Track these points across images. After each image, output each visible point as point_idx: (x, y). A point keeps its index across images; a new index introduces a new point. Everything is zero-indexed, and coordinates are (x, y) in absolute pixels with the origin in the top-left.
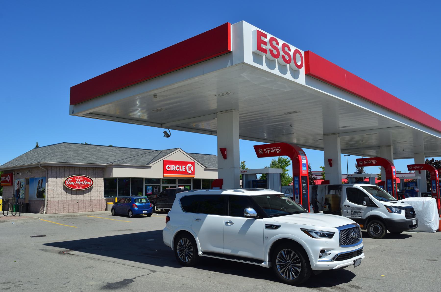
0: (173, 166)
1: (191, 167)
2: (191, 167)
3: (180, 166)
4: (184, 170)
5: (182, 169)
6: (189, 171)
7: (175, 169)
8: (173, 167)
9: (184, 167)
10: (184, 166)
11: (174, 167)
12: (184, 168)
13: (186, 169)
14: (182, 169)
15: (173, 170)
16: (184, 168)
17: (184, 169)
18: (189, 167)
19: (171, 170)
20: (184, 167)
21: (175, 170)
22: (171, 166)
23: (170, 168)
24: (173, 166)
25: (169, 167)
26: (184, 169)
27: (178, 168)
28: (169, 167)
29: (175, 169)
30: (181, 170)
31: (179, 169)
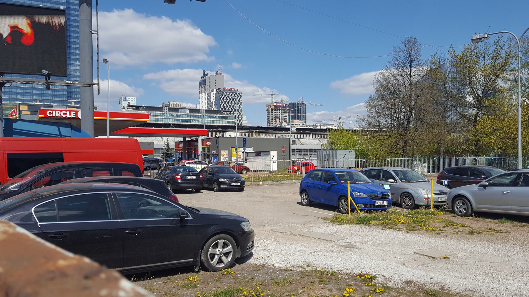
4: (75, 116)
5: (70, 114)
7: (60, 115)
9: (74, 113)
11: (58, 113)
12: (75, 114)
14: (70, 114)
15: (57, 116)
16: (75, 114)
17: (74, 115)
19: (54, 115)
20: (74, 113)
21: (60, 116)
23: (53, 114)
25: (50, 113)
26: (74, 115)
28: (50, 113)
29: (60, 115)
30: (70, 116)
31: (67, 115)
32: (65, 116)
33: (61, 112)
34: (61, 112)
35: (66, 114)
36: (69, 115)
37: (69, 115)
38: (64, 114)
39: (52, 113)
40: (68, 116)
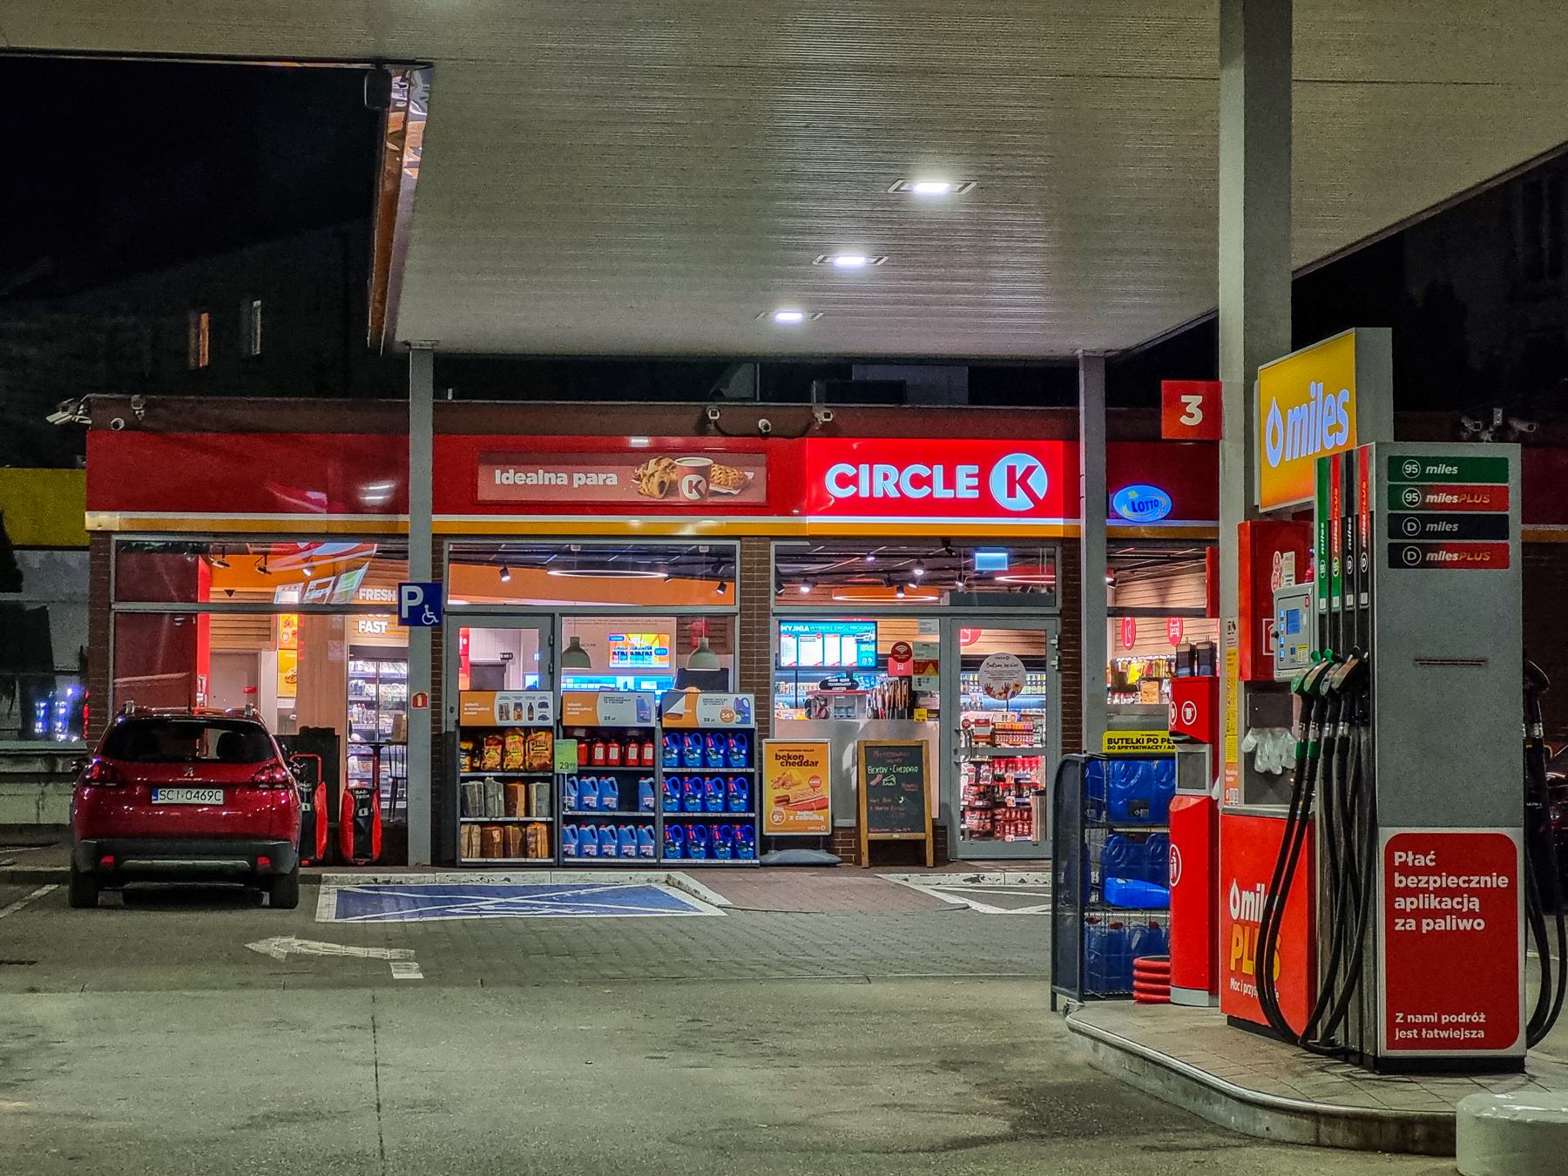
0: (879, 469)
1: (1030, 470)
2: (1030, 470)
3: (939, 471)
4: (975, 494)
5: (950, 482)
6: (1011, 493)
7: (897, 485)
8: (878, 478)
9: (968, 476)
10: (975, 469)
11: (886, 477)
12: (975, 482)
13: (984, 486)
14: (950, 482)
15: (878, 494)
16: (975, 482)
17: (969, 488)
18: (1011, 470)
19: (864, 493)
21: (893, 493)
22: (864, 468)
23: (856, 484)
24: (876, 466)
25: (843, 481)
26: (969, 488)
27: (917, 481)
28: (843, 481)
29: (897, 485)
30: (949, 494)
31: (931, 486)
32: (925, 491)
33: (901, 470)
34: (901, 470)
35: (928, 481)
36: (945, 487)
37: (945, 487)
38: (917, 481)
39: (854, 480)
40: (940, 492)
